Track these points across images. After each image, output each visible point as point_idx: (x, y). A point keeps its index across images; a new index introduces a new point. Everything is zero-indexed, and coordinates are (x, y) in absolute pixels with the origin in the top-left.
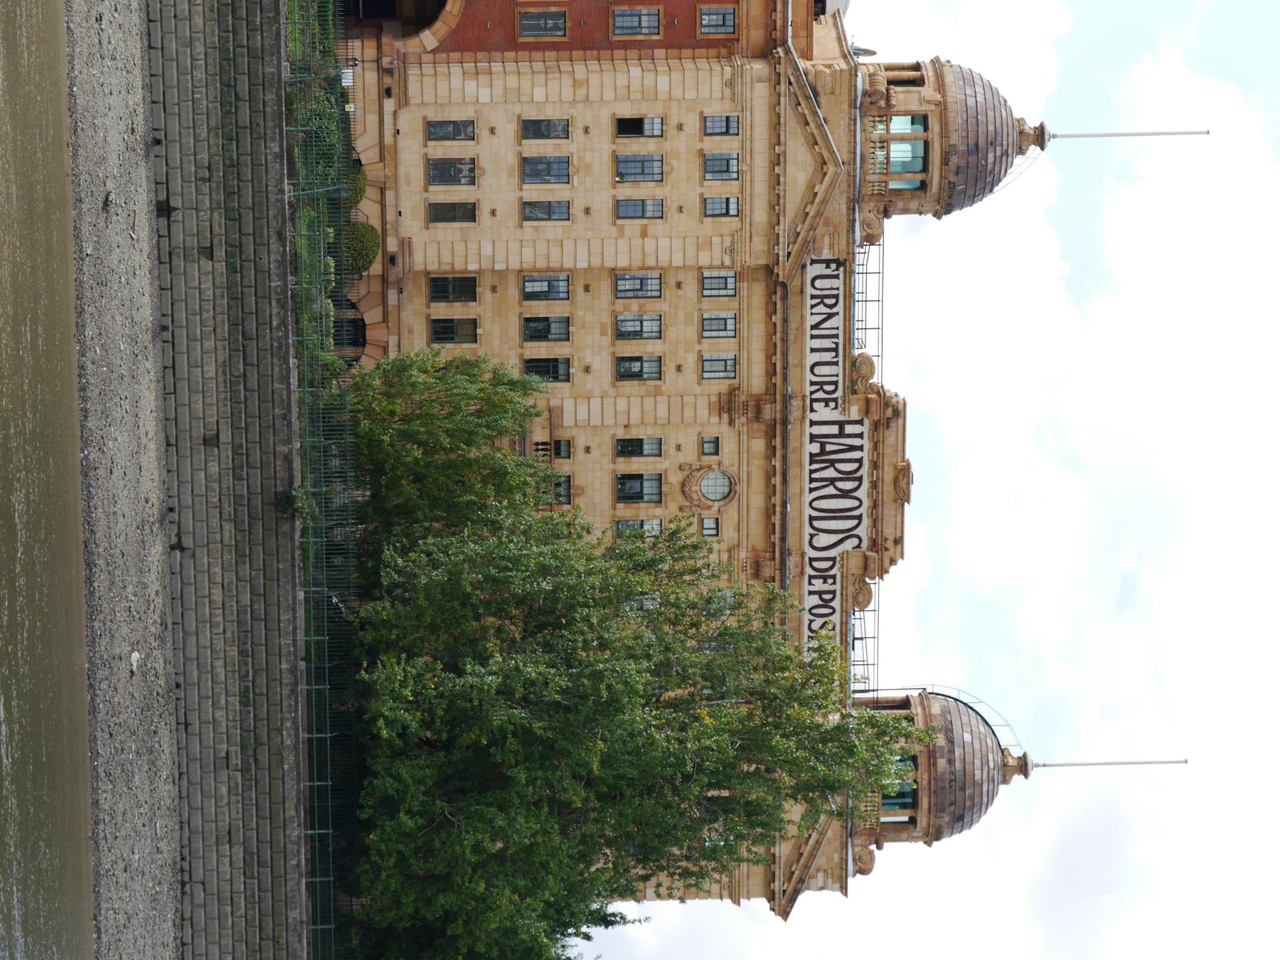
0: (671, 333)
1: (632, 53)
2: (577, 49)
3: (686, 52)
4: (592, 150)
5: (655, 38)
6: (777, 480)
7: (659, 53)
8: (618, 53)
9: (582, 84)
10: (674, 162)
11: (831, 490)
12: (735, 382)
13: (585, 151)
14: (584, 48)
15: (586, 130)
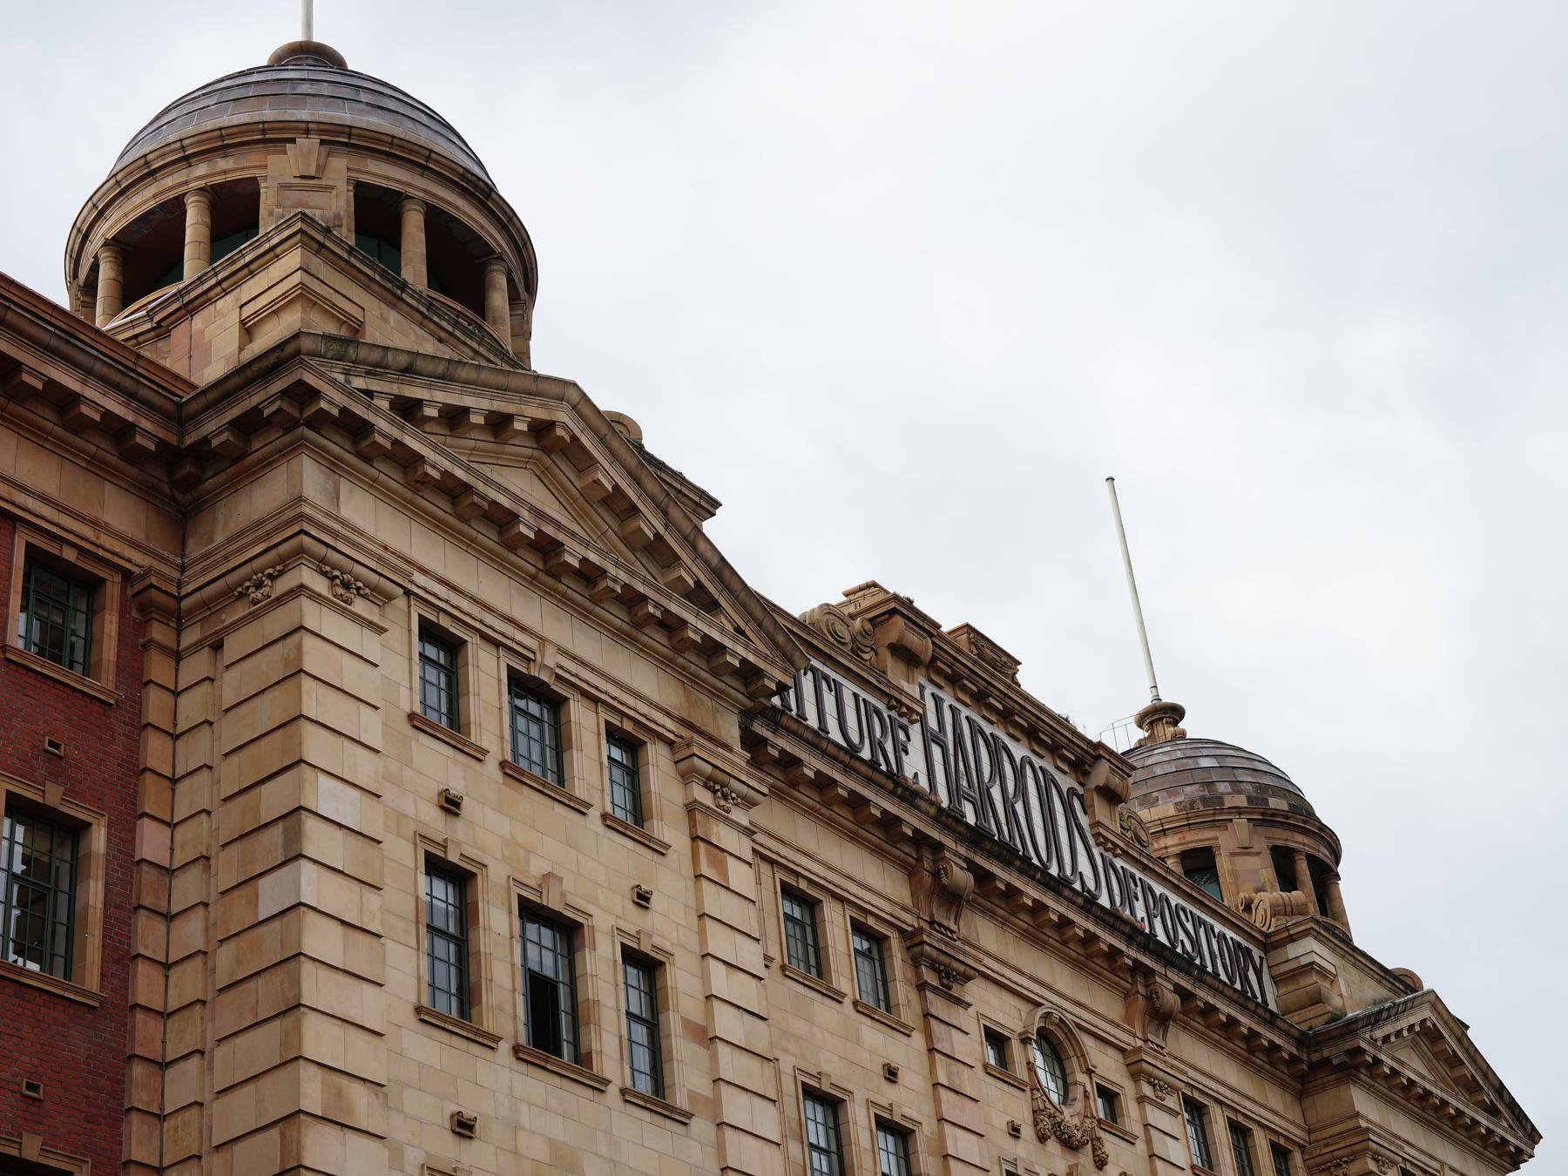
0: (835, 1072)
1: (148, 936)
2: (117, 1140)
3: (155, 751)
4: (517, 1128)
5: (98, 839)
6: (1056, 907)
7: (151, 842)
8: (146, 986)
9: (339, 1093)
10: (537, 867)
11: (1019, 807)
12: (895, 943)
13: (515, 1153)
14: (118, 1112)
15: (463, 1127)
